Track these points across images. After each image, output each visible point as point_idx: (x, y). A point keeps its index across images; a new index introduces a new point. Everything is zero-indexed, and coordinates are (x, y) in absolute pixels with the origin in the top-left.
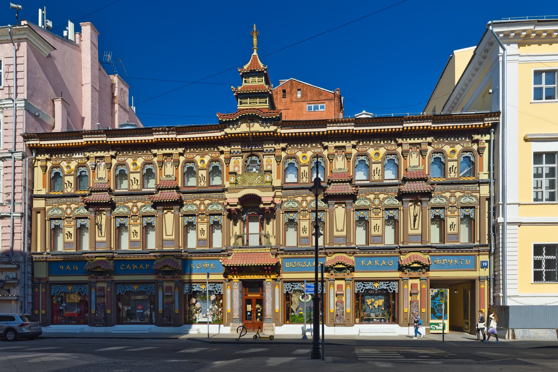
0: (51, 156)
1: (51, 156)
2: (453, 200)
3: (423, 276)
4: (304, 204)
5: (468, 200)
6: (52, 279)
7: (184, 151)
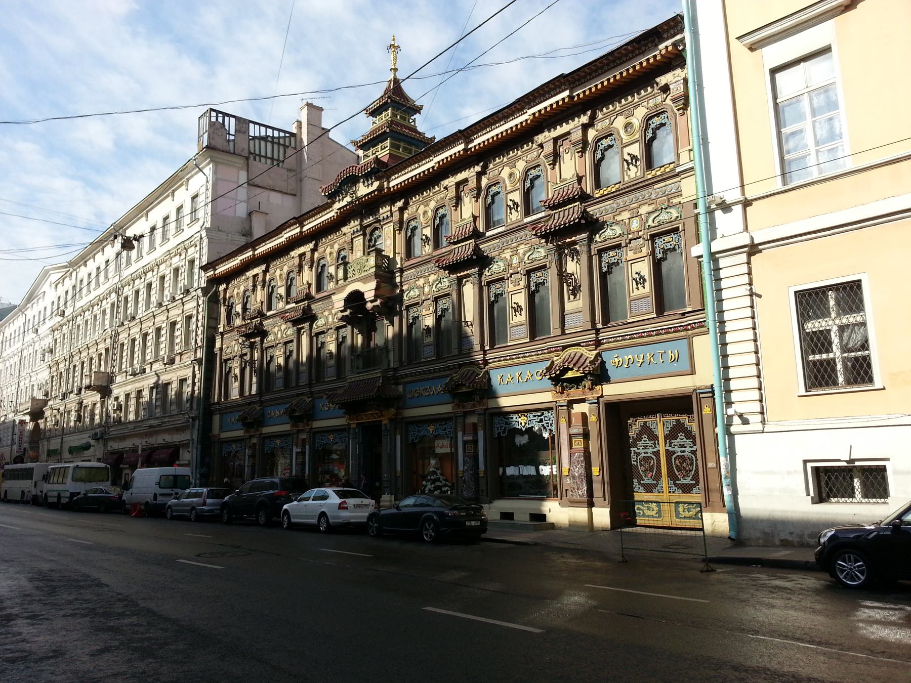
0: (227, 286)
1: (227, 286)
2: (635, 225)
3: (591, 396)
4: (427, 289)
5: (664, 217)
6: (224, 435)
7: (316, 246)
